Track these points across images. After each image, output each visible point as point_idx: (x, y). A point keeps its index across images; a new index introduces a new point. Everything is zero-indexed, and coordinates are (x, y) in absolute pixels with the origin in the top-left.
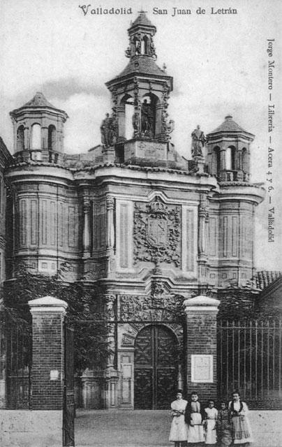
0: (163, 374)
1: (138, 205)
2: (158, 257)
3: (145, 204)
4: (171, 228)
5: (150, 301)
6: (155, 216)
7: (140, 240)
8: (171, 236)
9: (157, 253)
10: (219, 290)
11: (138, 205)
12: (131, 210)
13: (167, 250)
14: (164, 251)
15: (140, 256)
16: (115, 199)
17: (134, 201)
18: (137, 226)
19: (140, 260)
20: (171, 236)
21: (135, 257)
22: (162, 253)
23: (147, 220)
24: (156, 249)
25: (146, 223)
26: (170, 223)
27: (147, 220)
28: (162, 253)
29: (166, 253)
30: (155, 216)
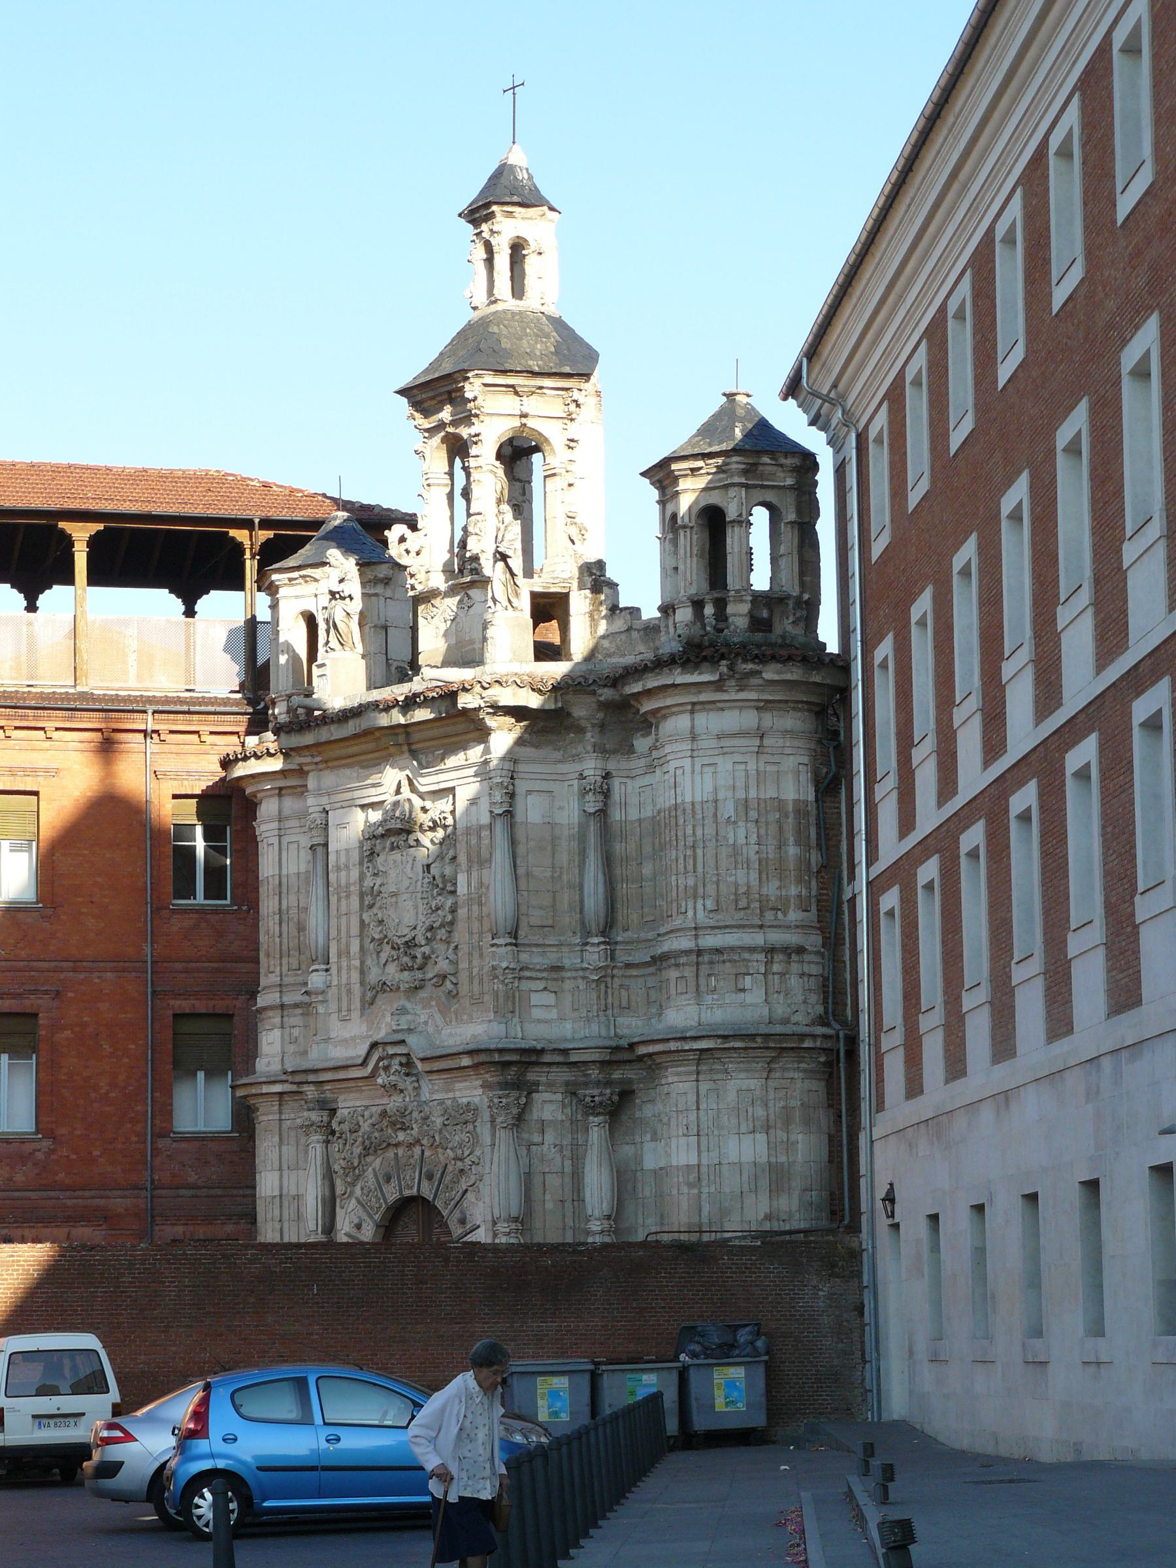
18: (368, 882)
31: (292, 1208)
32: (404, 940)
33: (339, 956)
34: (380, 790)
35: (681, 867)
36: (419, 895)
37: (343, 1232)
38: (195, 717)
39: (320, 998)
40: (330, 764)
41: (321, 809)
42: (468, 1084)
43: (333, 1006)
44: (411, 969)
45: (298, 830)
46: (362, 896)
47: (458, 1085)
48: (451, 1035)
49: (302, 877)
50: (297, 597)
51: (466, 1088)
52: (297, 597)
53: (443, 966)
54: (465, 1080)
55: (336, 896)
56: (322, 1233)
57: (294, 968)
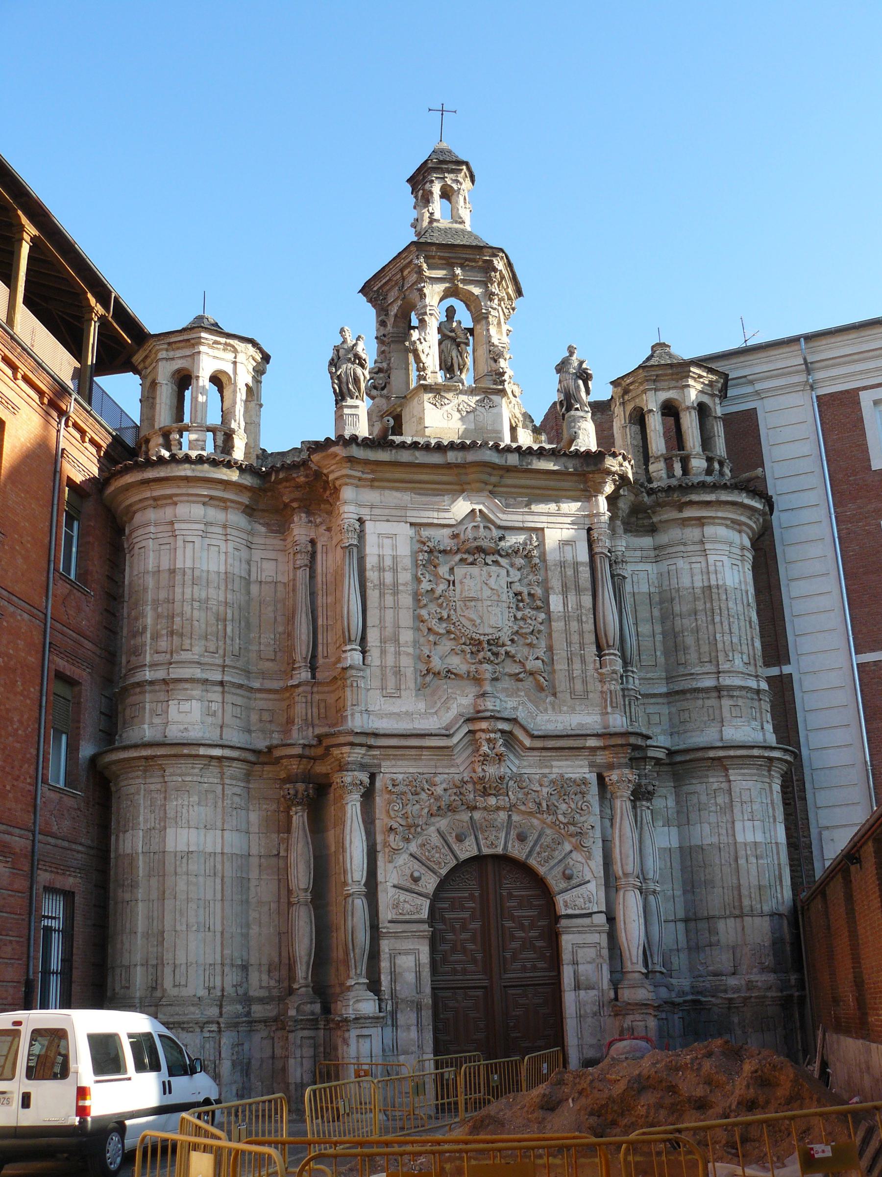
0: (521, 1001)
1: (425, 533)
2: (486, 666)
3: (447, 532)
4: (517, 587)
5: (470, 787)
6: (471, 559)
7: (434, 623)
8: (518, 609)
9: (481, 655)
10: (671, 753)
11: (425, 533)
12: (404, 550)
13: (511, 649)
14: (502, 650)
15: (437, 664)
16: (361, 521)
17: (411, 524)
18: (425, 586)
19: (437, 674)
20: (518, 609)
21: (423, 667)
22: (496, 655)
23: (452, 570)
24: (480, 643)
25: (452, 578)
26: (515, 575)
27: (452, 570)
28: (496, 655)
29: (507, 653)
30: (471, 559)
31: (207, 864)
32: (487, 638)
33: (383, 641)
34: (446, 515)
35: (726, 628)
36: (505, 605)
37: (389, 884)
38: (91, 420)
39: (361, 674)
40: (376, 484)
41: (357, 517)
42: (568, 763)
43: (376, 683)
44: (489, 662)
45: (220, 537)
46: (417, 597)
47: (554, 763)
48: (549, 721)
49: (223, 576)
50: (214, 357)
51: (568, 766)
52: (214, 357)
53: (531, 665)
54: (567, 760)
55: (377, 592)
56: (364, 885)
57: (211, 650)
